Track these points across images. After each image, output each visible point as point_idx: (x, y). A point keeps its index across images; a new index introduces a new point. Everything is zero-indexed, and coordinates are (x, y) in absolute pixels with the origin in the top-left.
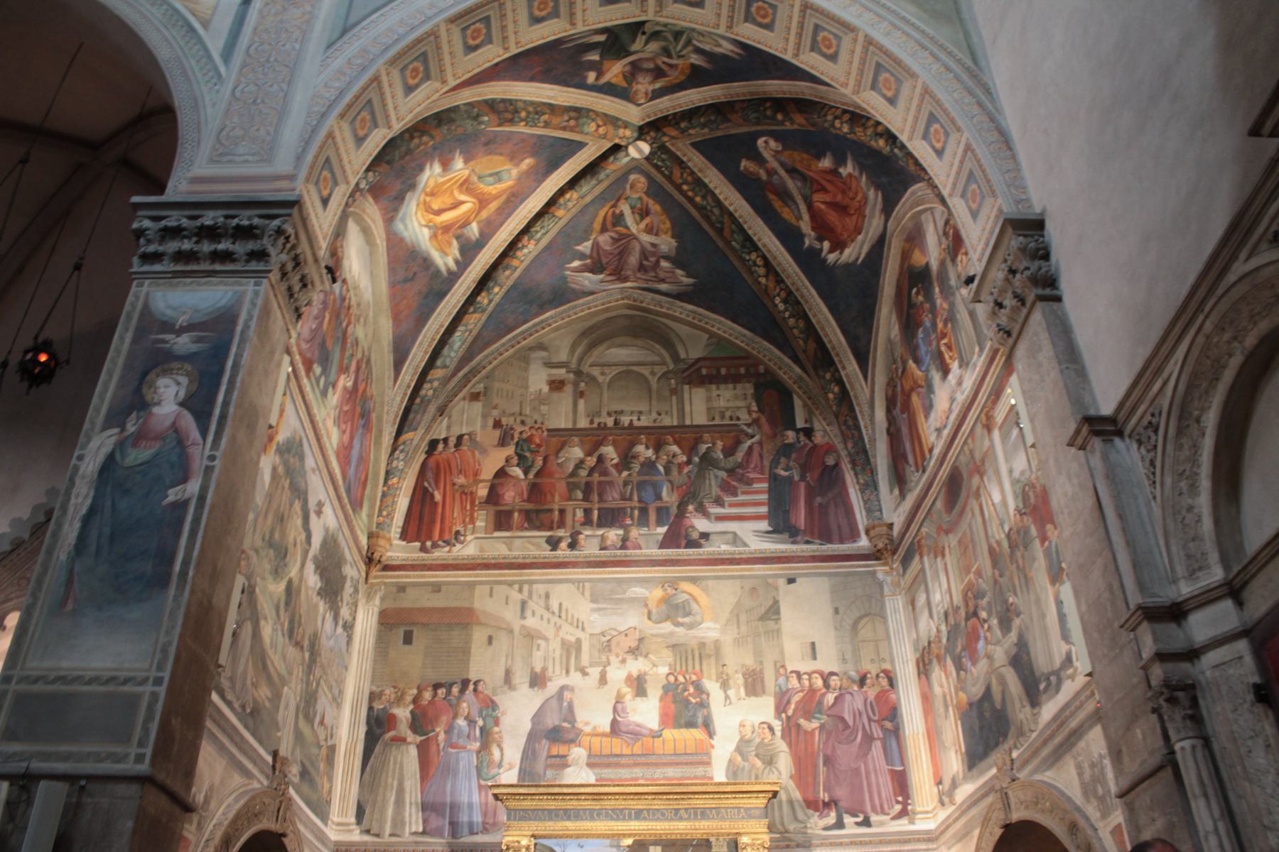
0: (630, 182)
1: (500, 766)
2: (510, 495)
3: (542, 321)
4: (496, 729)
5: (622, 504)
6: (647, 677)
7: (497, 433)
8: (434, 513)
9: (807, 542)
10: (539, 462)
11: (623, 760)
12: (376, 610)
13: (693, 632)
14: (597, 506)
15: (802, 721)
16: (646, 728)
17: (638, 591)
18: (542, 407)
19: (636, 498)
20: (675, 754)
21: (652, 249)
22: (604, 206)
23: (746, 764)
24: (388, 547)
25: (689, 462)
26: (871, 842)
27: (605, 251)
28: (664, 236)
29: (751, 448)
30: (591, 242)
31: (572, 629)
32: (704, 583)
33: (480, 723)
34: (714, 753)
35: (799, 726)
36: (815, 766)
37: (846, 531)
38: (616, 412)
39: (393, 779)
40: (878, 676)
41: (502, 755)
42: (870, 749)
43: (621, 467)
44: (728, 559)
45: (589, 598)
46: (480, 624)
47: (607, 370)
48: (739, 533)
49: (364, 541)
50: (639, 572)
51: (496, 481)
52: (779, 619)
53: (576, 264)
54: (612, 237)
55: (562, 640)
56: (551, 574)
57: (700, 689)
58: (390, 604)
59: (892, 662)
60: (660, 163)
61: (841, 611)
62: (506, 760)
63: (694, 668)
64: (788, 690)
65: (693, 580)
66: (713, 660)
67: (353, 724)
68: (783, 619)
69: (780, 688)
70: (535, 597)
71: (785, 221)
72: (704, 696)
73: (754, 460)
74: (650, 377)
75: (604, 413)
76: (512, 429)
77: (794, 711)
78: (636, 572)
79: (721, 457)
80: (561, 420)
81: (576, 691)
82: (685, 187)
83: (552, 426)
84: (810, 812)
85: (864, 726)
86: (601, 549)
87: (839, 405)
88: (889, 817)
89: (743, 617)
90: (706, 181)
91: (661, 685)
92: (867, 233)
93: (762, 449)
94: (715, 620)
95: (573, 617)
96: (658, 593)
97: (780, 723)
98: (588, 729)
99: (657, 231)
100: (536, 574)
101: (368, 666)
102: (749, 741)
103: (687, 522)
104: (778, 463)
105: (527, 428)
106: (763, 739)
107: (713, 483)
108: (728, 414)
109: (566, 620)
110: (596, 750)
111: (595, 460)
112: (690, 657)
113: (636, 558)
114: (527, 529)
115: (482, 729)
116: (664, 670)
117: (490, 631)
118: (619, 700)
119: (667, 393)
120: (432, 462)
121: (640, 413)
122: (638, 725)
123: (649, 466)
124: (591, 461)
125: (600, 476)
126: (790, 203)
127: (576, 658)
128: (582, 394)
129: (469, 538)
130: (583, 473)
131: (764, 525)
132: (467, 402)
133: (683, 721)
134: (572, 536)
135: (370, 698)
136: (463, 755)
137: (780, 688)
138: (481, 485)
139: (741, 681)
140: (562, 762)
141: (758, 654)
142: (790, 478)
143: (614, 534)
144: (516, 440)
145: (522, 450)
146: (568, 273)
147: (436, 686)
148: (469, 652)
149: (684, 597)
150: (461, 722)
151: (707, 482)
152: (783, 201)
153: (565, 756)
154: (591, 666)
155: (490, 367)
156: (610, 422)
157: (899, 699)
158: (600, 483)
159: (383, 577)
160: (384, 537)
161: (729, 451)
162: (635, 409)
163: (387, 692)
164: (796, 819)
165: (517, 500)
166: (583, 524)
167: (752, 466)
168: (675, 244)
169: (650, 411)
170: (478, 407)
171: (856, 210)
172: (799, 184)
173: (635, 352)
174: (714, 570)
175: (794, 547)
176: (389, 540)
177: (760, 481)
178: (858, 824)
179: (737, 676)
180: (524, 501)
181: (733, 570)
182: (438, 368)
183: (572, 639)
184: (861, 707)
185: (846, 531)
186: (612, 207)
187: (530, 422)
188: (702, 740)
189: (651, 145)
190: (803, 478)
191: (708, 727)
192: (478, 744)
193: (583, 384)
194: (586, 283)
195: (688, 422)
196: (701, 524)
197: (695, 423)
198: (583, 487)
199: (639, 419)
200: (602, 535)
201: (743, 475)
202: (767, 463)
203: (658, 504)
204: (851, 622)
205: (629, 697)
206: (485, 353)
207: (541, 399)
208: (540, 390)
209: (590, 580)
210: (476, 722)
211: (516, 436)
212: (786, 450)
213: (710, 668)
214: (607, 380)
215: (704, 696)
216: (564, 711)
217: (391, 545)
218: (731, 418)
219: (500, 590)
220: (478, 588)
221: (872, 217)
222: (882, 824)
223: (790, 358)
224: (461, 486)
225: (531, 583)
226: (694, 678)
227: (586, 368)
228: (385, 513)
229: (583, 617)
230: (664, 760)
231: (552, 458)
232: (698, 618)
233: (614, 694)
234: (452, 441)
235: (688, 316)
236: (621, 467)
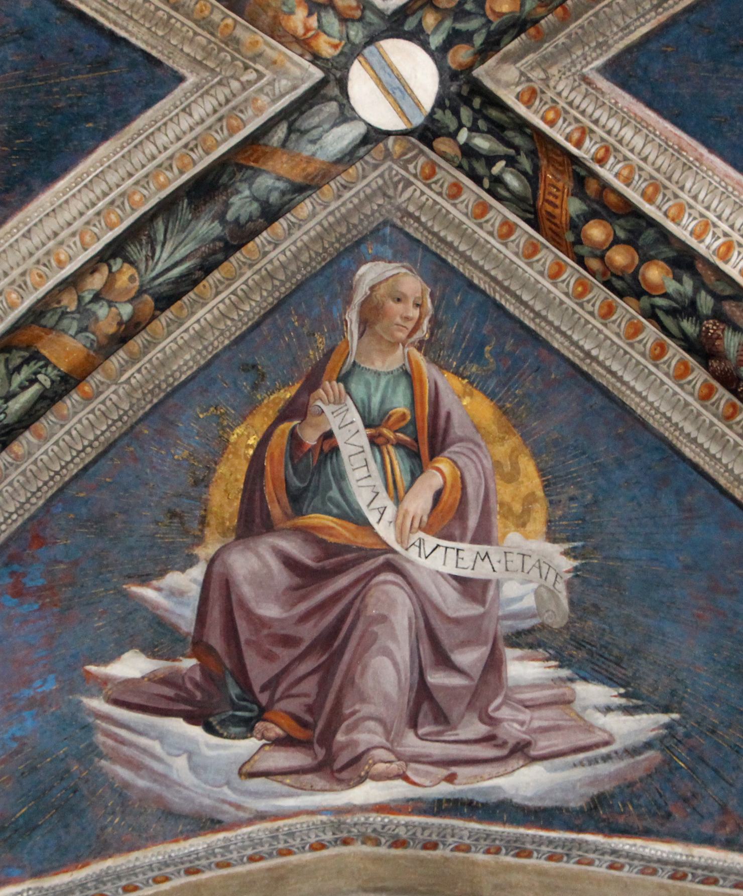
0: (358, 298)
21: (471, 610)
22: (251, 406)
27: (259, 623)
28: (514, 538)
30: (197, 572)
54: (290, 563)
60: (483, 143)
82: (596, 232)
99: (486, 514)
168: (567, 564)
186: (284, 416)
189: (439, 55)
194: (179, 767)
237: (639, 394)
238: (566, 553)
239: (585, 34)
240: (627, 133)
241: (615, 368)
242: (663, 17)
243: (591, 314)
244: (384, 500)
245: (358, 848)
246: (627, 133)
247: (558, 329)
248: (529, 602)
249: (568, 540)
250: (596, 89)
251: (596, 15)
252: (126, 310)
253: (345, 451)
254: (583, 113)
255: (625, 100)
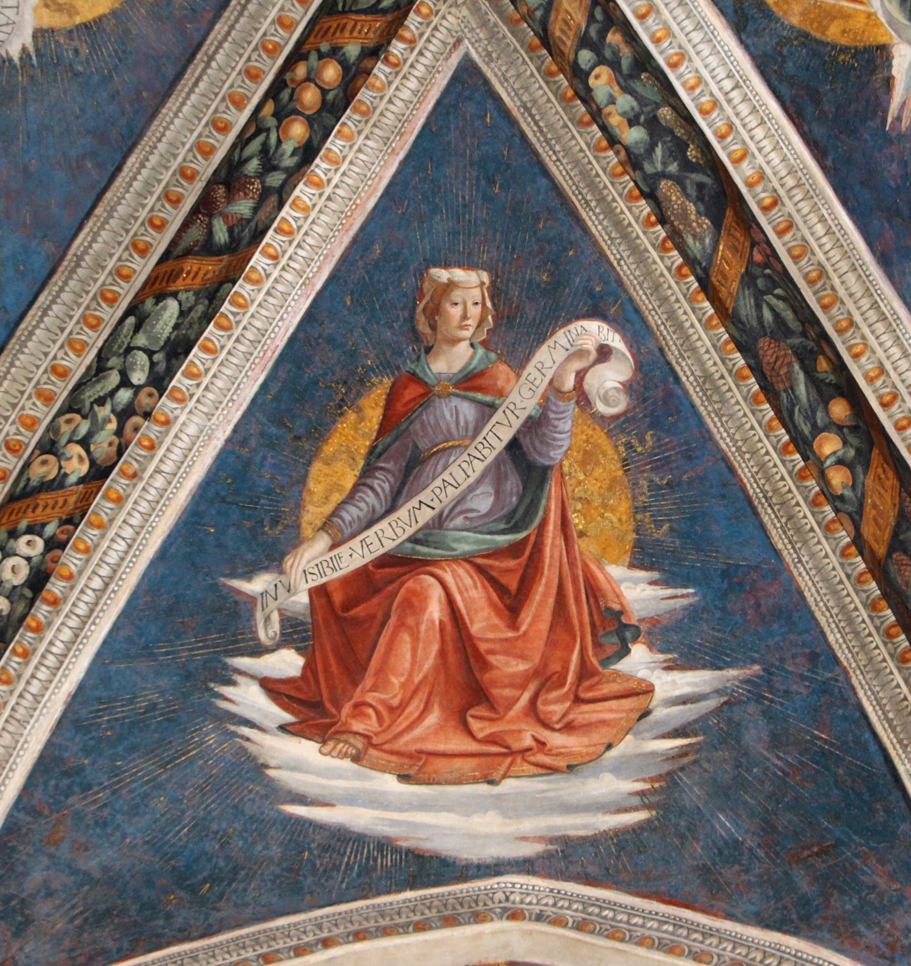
71: (303, 480)
82: (331, 73)
90: (334, 144)
92: (424, 806)
126: (382, 484)
152: (374, 455)
168: (14, 51)
171: (491, 740)
172: (483, 503)
221: (499, 804)
237: (179, 110)
238: (24, 49)
239: (499, 40)
240: (413, 84)
241: (202, 85)
242: (516, 113)
243: (249, 59)
246: (413, 84)
247: (232, 27)
249: (37, 50)
250: (451, 52)
251: (516, 50)
254: (428, 41)
255: (442, 81)
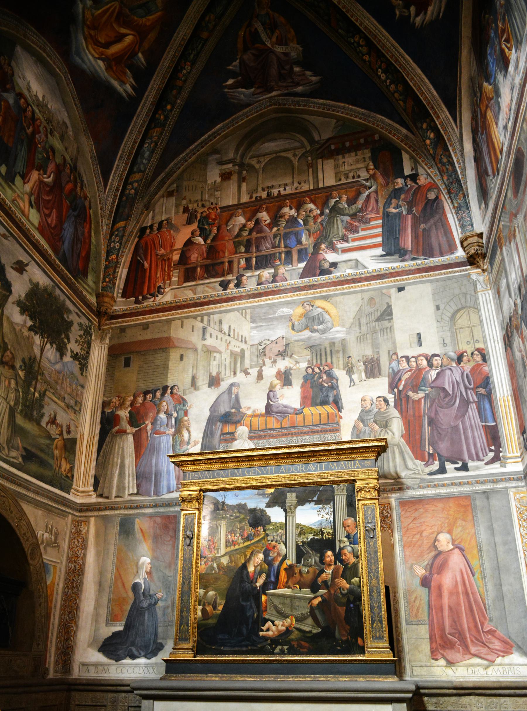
1: (188, 443)
2: (194, 257)
3: (214, 133)
4: (186, 418)
5: (272, 251)
6: (292, 371)
7: (186, 216)
8: (144, 276)
9: (414, 259)
10: (215, 230)
11: (275, 433)
12: (106, 346)
13: (326, 335)
14: (255, 255)
15: (410, 393)
16: (291, 408)
17: (285, 311)
18: (216, 193)
19: (283, 245)
20: (313, 425)
23: (367, 429)
24: (112, 303)
25: (322, 214)
26: (468, 483)
29: (368, 196)
31: (238, 344)
32: (333, 299)
33: (175, 415)
34: (342, 422)
35: (408, 397)
36: (421, 426)
37: (445, 247)
38: (268, 187)
39: (118, 459)
40: (472, 354)
41: (190, 436)
42: (467, 410)
43: (270, 226)
44: (352, 279)
45: (250, 320)
46: (175, 347)
47: (262, 159)
48: (359, 259)
49: (93, 300)
50: (286, 297)
51: (185, 249)
52: (392, 319)
53: (230, 82)
55: (231, 351)
56: (223, 307)
57: (330, 376)
58: (116, 341)
59: (485, 341)
61: (442, 307)
62: (193, 439)
63: (326, 361)
64: (399, 371)
65: (325, 298)
66: (341, 354)
67: (92, 425)
68: (394, 318)
69: (393, 370)
70: (212, 324)
72: (334, 381)
73: (371, 204)
74: (293, 159)
75: (260, 189)
76: (196, 211)
77: (404, 386)
78: (283, 298)
79: (346, 206)
80: (230, 200)
81: (241, 386)
83: (223, 205)
84: (418, 462)
85: (461, 392)
86: (258, 285)
87: (435, 148)
88: (484, 462)
89: (364, 321)
91: (302, 376)
93: (377, 196)
94: (343, 326)
95: (238, 334)
96: (300, 310)
97: (393, 396)
98: (249, 412)
100: (212, 308)
101: (101, 384)
102: (369, 411)
103: (321, 257)
104: (390, 203)
105: (206, 209)
106: (380, 409)
107: (340, 226)
108: (351, 175)
109: (234, 338)
110: (255, 426)
111: (253, 223)
112: (323, 354)
113: (283, 288)
114: (206, 278)
115: (176, 419)
116: (304, 365)
117: (181, 351)
118: (271, 390)
119: (306, 168)
120: (143, 241)
121: (286, 185)
122: (286, 407)
123: (293, 221)
124: (251, 224)
125: (257, 234)
127: (241, 363)
128: (244, 179)
129: (167, 290)
130: (245, 233)
131: (379, 251)
132: (165, 198)
133: (318, 401)
134: (237, 279)
135: (103, 405)
136: (164, 438)
137: (393, 370)
138: (175, 252)
139: (362, 367)
140: (231, 437)
141: (375, 346)
142: (400, 214)
143: (267, 273)
144: (199, 218)
145: (203, 224)
146: (226, 90)
147: (146, 393)
148: (168, 367)
149: (320, 310)
150: (162, 416)
151: (335, 226)
153: (233, 433)
154: (251, 368)
155: (179, 171)
156: (264, 195)
157: (491, 370)
158: (257, 238)
159: (111, 324)
160: (107, 296)
161: (351, 202)
162: (281, 183)
163: (114, 400)
164: (407, 468)
165: (199, 259)
166: (245, 269)
167: (370, 209)
169: (293, 182)
170: (172, 200)
173: (282, 142)
174: (341, 289)
175: (403, 264)
176: (113, 298)
177: (376, 219)
178: (457, 469)
179: (359, 364)
180: (203, 259)
181: (355, 287)
182: (135, 173)
183: (238, 350)
184: (459, 379)
185: (445, 247)
187: (207, 204)
188: (333, 414)
190: (410, 212)
191: (337, 404)
192: (173, 430)
193: (245, 172)
195: (321, 185)
196: (331, 257)
197: (326, 185)
198: (245, 244)
199: (285, 189)
200: (259, 275)
201: (362, 217)
202: (381, 206)
203: (300, 247)
204: (449, 315)
205: (278, 387)
206: (176, 161)
207: (216, 188)
208: (215, 182)
209: (249, 308)
210: (172, 415)
211: (199, 215)
212: (396, 193)
213: (339, 360)
214: (262, 166)
215: (334, 381)
216: (233, 401)
217: (115, 302)
218: (354, 177)
219: (188, 323)
220: (173, 323)
222: (477, 468)
223: (397, 123)
224: (162, 255)
225: (209, 315)
226: (327, 368)
227: (247, 161)
228: (107, 280)
229: (245, 334)
230: (305, 429)
231: (223, 226)
232: (329, 325)
233: (268, 386)
234: (156, 226)
235: (319, 108)
236: (270, 226)
244: (268, 39)
245: (273, 107)
248: (296, 56)
252: (214, 23)
253: (260, 31)
